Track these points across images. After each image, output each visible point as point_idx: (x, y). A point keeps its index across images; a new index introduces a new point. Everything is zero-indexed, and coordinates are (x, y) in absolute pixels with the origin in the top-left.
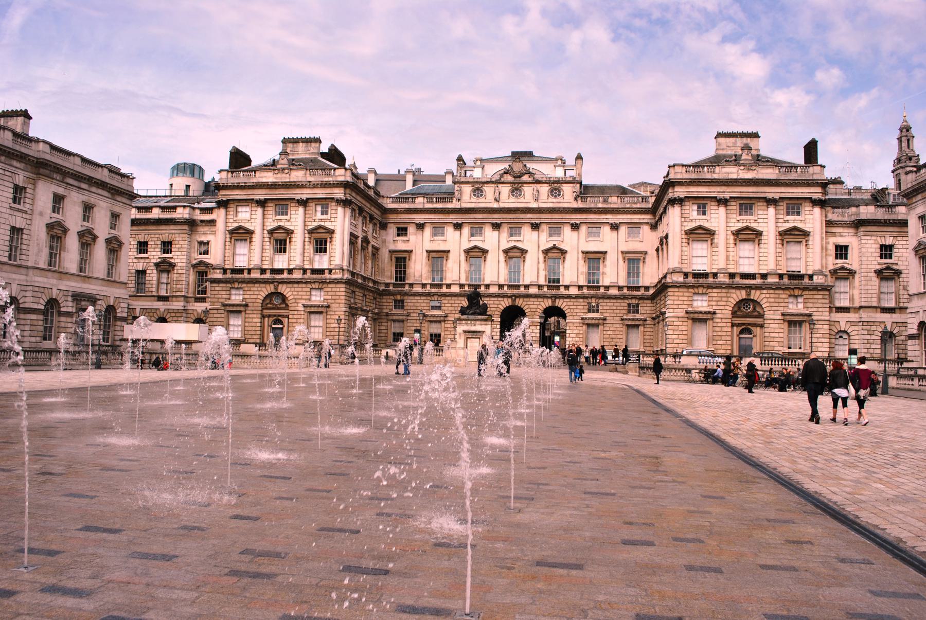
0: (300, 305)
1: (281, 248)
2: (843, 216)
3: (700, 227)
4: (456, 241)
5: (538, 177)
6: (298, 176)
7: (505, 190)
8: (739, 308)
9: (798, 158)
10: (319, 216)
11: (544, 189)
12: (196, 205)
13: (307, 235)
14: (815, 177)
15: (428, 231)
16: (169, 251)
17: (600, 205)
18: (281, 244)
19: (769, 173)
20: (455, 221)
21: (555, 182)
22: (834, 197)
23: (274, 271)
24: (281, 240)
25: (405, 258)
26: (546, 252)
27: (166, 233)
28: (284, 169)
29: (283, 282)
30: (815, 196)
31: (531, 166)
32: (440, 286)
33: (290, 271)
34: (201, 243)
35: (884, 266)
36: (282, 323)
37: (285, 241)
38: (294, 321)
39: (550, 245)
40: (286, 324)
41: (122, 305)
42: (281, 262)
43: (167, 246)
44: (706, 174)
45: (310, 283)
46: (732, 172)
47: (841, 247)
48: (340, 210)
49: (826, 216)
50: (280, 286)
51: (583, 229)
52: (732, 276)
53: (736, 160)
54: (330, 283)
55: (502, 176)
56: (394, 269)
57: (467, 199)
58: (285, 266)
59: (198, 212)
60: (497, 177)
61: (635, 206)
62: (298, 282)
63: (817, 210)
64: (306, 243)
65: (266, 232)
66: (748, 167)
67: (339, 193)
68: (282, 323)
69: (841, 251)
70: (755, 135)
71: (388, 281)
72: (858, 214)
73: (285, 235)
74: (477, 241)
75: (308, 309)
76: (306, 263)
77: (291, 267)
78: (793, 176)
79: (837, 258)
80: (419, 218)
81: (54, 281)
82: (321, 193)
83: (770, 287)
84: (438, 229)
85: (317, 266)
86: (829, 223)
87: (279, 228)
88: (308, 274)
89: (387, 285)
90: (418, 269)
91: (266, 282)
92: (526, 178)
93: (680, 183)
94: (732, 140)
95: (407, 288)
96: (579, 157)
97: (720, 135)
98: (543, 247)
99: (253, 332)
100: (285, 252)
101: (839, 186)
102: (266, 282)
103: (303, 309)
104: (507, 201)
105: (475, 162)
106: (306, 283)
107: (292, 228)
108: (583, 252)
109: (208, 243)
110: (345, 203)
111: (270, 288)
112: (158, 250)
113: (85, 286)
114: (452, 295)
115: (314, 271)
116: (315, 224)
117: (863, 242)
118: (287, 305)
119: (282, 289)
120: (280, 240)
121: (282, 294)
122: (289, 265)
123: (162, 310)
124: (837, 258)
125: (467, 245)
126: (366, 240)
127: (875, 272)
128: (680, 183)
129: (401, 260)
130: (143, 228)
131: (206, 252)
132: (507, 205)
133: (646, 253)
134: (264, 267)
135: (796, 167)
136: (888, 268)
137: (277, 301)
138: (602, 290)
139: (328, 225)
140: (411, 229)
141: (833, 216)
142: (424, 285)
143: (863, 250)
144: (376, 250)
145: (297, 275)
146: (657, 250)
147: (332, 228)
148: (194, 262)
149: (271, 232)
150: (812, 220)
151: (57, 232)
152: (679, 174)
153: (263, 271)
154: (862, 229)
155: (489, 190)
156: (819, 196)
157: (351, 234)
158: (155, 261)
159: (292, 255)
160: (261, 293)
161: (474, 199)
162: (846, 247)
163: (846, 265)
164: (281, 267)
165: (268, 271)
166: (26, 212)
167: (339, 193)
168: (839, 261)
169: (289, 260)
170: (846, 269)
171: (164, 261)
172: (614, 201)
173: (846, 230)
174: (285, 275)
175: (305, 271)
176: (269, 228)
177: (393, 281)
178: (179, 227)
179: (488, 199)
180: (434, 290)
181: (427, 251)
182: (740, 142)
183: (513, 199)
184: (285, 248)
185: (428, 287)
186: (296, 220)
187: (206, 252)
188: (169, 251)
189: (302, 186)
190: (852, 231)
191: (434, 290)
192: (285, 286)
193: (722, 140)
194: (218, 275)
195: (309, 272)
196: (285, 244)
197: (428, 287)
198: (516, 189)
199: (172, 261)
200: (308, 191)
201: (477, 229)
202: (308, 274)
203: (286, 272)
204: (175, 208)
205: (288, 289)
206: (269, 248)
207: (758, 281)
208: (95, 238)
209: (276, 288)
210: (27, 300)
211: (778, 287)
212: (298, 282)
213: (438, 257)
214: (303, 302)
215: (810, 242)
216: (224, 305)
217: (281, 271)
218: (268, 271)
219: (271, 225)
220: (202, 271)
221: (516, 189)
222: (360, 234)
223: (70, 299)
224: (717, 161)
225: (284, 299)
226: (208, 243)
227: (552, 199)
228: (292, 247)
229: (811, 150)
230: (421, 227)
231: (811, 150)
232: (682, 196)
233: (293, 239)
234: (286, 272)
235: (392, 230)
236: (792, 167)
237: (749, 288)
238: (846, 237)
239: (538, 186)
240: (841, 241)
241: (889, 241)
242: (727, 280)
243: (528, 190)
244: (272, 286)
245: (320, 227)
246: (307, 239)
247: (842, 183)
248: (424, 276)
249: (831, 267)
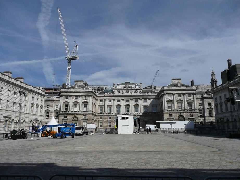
1: (76, 106)
2: (200, 96)
3: (170, 100)
4: (114, 103)
5: (132, 88)
6: (79, 90)
7: (125, 91)
8: (179, 117)
9: (190, 85)
10: (84, 98)
11: (133, 91)
12: (55, 96)
15: (107, 101)
17: (146, 94)
19: (184, 88)
20: (113, 99)
21: (136, 89)
24: (76, 104)
25: (102, 107)
26: (134, 105)
27: (48, 103)
28: (77, 88)
29: (77, 114)
31: (130, 85)
32: (111, 114)
34: (56, 105)
35: (210, 107)
39: (136, 104)
41: (43, 121)
43: (48, 106)
44: (171, 89)
45: (83, 114)
46: (175, 88)
48: (90, 97)
51: (143, 100)
52: (177, 110)
53: (176, 85)
54: (88, 114)
55: (124, 88)
56: (100, 110)
57: (116, 93)
59: (55, 98)
60: (123, 88)
61: (154, 94)
66: (179, 87)
67: (90, 94)
70: (180, 79)
71: (98, 113)
74: (119, 103)
75: (83, 120)
78: (189, 88)
80: (105, 98)
81: (32, 116)
82: (85, 94)
83: (185, 113)
84: (110, 101)
86: (197, 98)
89: (98, 114)
90: (106, 110)
91: (73, 114)
92: (129, 89)
93: (165, 91)
94: (175, 80)
95: (103, 114)
96: (141, 83)
97: (173, 79)
98: (134, 104)
102: (73, 114)
104: (125, 93)
105: (117, 85)
106: (82, 114)
108: (143, 105)
109: (58, 105)
110: (91, 96)
111: (74, 116)
113: (37, 117)
114: (113, 116)
115: (84, 111)
116: (84, 101)
119: (76, 116)
120: (76, 104)
123: (47, 121)
125: (117, 104)
126: (94, 104)
127: (207, 109)
128: (165, 91)
129: (101, 107)
131: (58, 107)
132: (125, 95)
133: (157, 105)
135: (189, 87)
136: (210, 108)
137: (75, 118)
138: (148, 114)
140: (103, 101)
142: (107, 114)
144: (96, 105)
145: (80, 112)
146: (160, 104)
148: (55, 110)
149: (73, 103)
151: (33, 104)
152: (165, 88)
155: (121, 91)
156: (195, 93)
157: (92, 103)
161: (118, 93)
166: (27, 101)
167: (90, 94)
172: (150, 94)
174: (77, 113)
177: (100, 113)
179: (120, 94)
180: (109, 115)
181: (107, 106)
182: (177, 81)
183: (127, 93)
184: (77, 106)
185: (108, 114)
186: (81, 100)
187: (58, 107)
189: (81, 92)
191: (109, 115)
193: (173, 80)
196: (77, 105)
197: (108, 114)
198: (128, 91)
200: (82, 93)
201: (119, 101)
204: (50, 97)
207: (183, 111)
208: (38, 106)
210: (27, 121)
211: (187, 113)
213: (110, 107)
214: (82, 119)
216: (62, 120)
220: (57, 112)
221: (128, 91)
222: (93, 102)
223: (34, 120)
224: (173, 85)
226: (58, 105)
227: (136, 93)
229: (192, 83)
230: (105, 100)
231: (192, 83)
232: (165, 93)
235: (99, 101)
236: (189, 87)
237: (180, 113)
239: (132, 90)
241: (210, 102)
242: (176, 111)
243: (130, 91)
248: (107, 111)
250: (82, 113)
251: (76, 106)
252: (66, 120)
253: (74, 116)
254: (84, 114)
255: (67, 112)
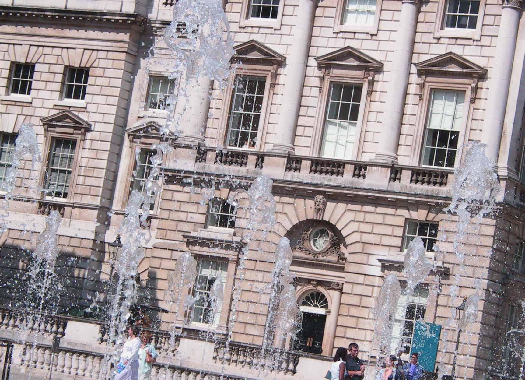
0: (373, 260)
1: (345, 107)
13: (414, 79)
16: (78, 92)
18: (347, 97)
23: (320, 165)
24: (348, 87)
33: (360, 168)
36: (321, 300)
37: (359, 88)
38: (355, 300)
40: (333, 306)
42: (341, 142)
43: (76, 80)
50: (330, 205)
58: (349, 157)
62: (377, 200)
64: (410, 99)
65: (312, 62)
68: (321, 300)
73: (359, 73)
76: (402, 150)
77: (365, 158)
85: (328, 154)
87: (348, 53)
88: (406, 181)
99: (249, 319)
100: (354, 117)
103: (377, 271)
106: (396, 204)
107: (377, 56)
111: (305, 209)
112: (58, 86)
118: (342, 257)
119: (335, 213)
121: (333, 228)
122: (360, 151)
130: (27, 30)
134: (299, 152)
139: (470, 54)
147: (481, 62)
149: (327, 63)
153: (293, 162)
158: (45, 113)
159: (371, 127)
160: (282, 218)
164: (340, 156)
165: (306, 164)
169: (362, 141)
171: (63, 117)
174: (347, 178)
175: (396, 172)
176: (322, 52)
178: (112, 35)
184: (356, 109)
188: (78, 92)
192: (342, 206)
194: (185, 162)
195: (406, 175)
196: (358, 98)
199: (83, 116)
202: (406, 181)
203: (349, 169)
205: (350, 216)
206: (316, 102)
209: (320, 210)
212: (377, 200)
216: (191, 241)
217: (336, 167)
218: (306, 164)
219: (327, 44)
225: (338, 240)
228: (374, 106)
233: (378, 86)
234: (349, 169)
244: (310, 203)
245: (450, 59)
246: (413, 89)
250: (396, 186)
251: (346, 103)
252: (220, 244)
253: (305, 209)
254: (417, 206)
255: (239, 158)
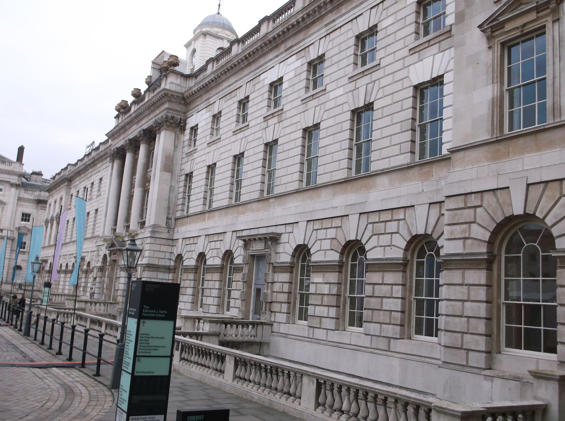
14: (15, 170)
22: (34, 183)
30: (12, 181)
47: (26, 215)
49: (19, 194)
63: (13, 190)
69: (26, 216)
72: (40, 195)
79: (22, 220)
86: (19, 199)
101: (40, 177)
117: (39, 213)
124: (22, 220)
141: (24, 195)
143: (39, 218)
150: (10, 195)
154: (40, 205)
162: (29, 215)
163: (27, 226)
168: (24, 223)
170: (27, 228)
173: (31, 205)
190: (35, 205)
215: (5, 209)
238: (29, 209)
240: (27, 211)
247: (42, 175)
249: (17, 226)
